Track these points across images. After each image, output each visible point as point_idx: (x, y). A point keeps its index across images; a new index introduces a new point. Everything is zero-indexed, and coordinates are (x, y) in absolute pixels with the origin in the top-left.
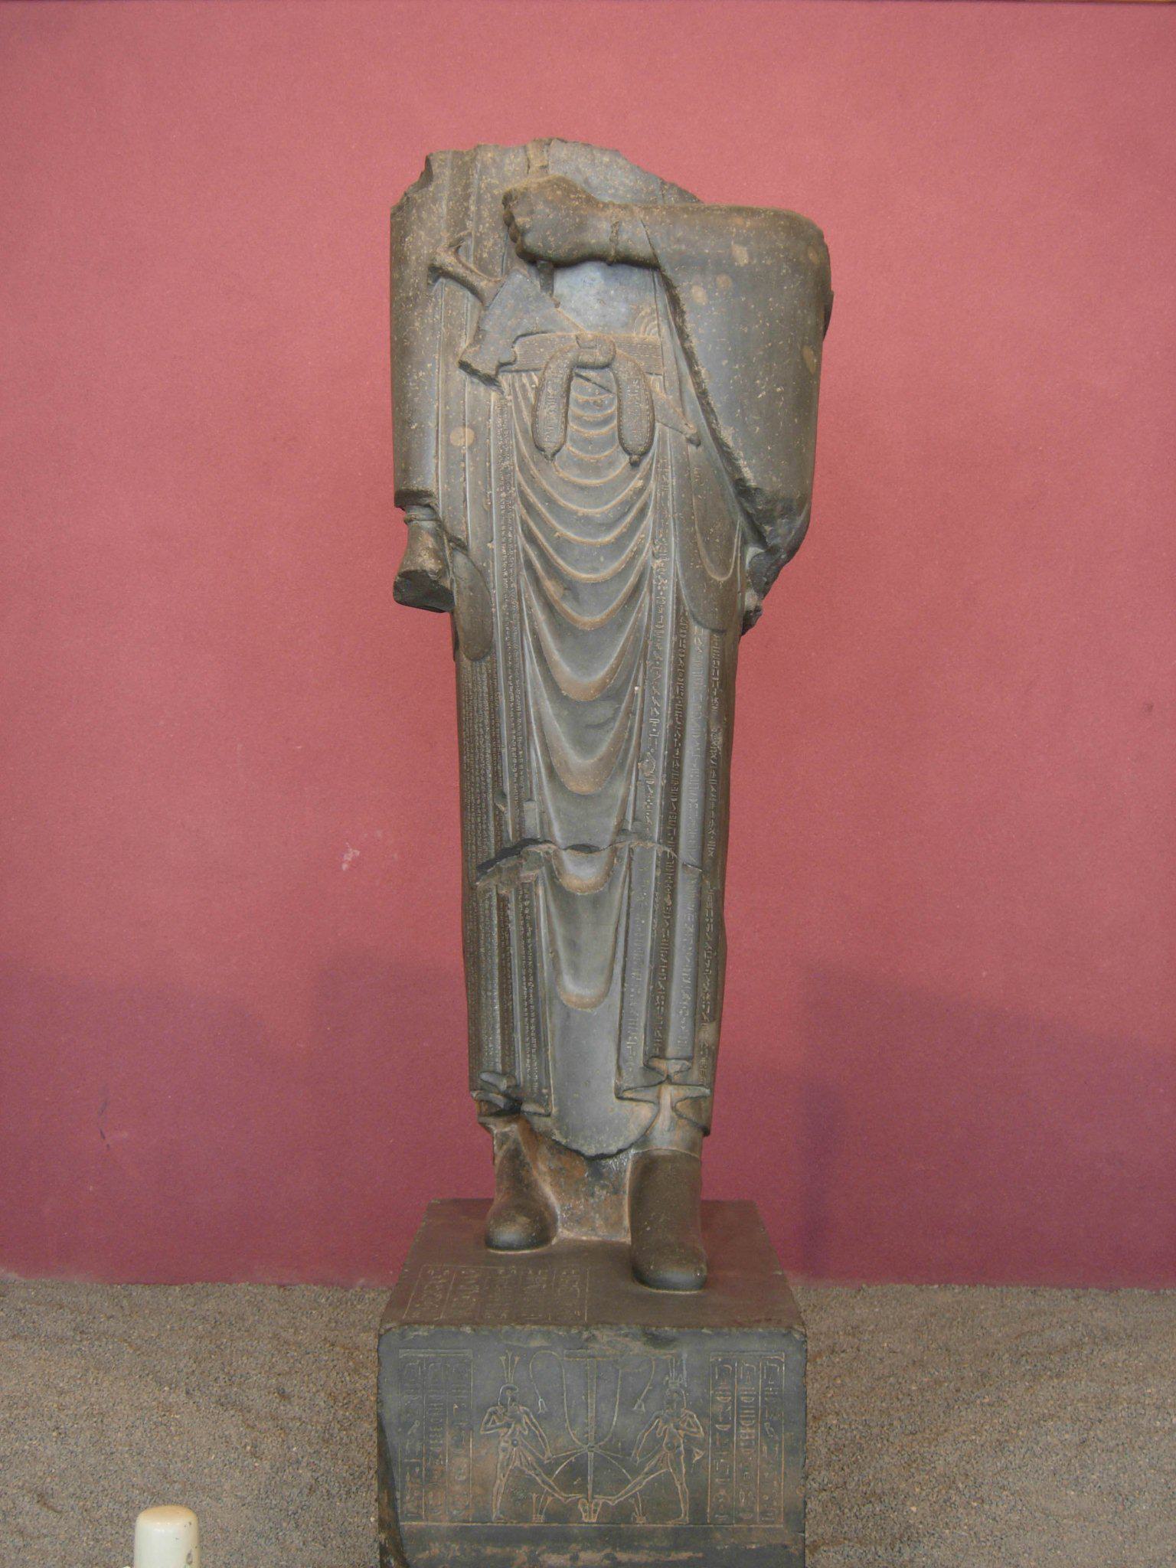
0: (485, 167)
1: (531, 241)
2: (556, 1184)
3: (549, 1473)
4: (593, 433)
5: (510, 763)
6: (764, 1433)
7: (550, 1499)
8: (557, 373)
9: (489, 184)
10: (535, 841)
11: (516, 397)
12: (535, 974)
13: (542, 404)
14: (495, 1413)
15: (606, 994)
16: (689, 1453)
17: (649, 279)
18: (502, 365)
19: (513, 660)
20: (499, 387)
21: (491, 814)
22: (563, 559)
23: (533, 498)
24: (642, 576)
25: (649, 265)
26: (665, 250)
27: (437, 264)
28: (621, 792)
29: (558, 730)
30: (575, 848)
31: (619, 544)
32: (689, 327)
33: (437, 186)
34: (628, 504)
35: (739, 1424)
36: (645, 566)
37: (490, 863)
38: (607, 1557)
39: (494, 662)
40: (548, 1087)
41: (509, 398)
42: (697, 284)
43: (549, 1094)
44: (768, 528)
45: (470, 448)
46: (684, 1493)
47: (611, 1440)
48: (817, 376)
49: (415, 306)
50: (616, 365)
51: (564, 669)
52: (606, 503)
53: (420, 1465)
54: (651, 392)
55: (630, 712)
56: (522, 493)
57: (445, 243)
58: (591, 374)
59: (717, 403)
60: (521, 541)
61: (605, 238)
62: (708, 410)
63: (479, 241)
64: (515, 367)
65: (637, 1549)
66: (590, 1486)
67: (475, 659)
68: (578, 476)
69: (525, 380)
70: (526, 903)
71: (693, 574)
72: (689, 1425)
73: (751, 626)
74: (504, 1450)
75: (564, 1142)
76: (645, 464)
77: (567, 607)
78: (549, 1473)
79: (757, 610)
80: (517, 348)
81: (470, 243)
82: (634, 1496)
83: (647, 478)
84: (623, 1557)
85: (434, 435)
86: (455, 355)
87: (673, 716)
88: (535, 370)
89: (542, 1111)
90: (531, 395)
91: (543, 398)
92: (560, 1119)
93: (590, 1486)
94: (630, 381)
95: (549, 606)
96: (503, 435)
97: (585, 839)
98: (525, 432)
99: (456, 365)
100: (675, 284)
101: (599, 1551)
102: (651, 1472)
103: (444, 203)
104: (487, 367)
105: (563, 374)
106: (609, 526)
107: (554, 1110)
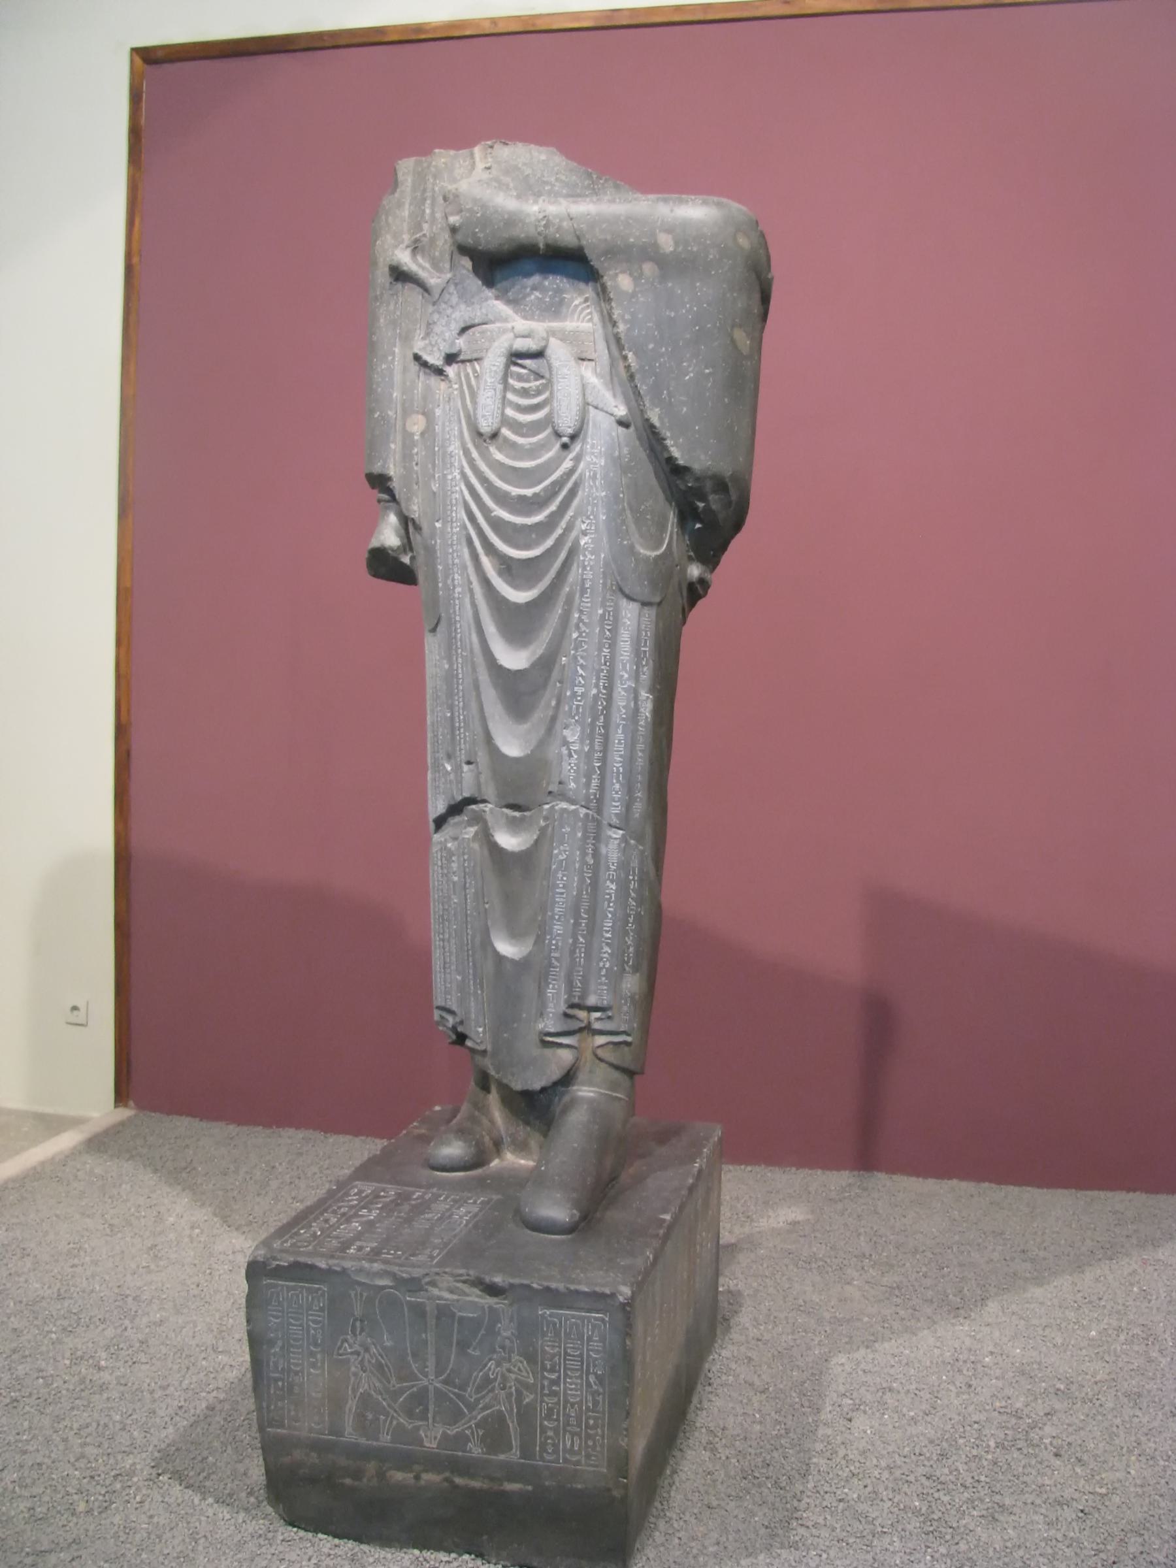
3: (395, 1401)
7: (395, 1423)
8: (494, 361)
20: (447, 376)
23: (474, 480)
27: (394, 263)
32: (616, 313)
35: (566, 1375)
38: (446, 1480)
41: (456, 386)
42: (623, 272)
44: (701, 505)
45: (422, 434)
50: (549, 352)
52: (540, 483)
53: (283, 1380)
58: (527, 362)
61: (532, 232)
63: (433, 240)
64: (462, 357)
65: (472, 1476)
68: (514, 458)
69: (469, 370)
72: (519, 1369)
74: (355, 1374)
76: (576, 448)
79: (703, 583)
83: (578, 459)
86: (411, 347)
88: (476, 360)
91: (482, 387)
93: (430, 1415)
97: (520, 801)
98: (468, 417)
99: (411, 357)
100: (601, 272)
101: (439, 1473)
102: (485, 1408)
103: (407, 206)
104: (435, 359)
105: (501, 361)
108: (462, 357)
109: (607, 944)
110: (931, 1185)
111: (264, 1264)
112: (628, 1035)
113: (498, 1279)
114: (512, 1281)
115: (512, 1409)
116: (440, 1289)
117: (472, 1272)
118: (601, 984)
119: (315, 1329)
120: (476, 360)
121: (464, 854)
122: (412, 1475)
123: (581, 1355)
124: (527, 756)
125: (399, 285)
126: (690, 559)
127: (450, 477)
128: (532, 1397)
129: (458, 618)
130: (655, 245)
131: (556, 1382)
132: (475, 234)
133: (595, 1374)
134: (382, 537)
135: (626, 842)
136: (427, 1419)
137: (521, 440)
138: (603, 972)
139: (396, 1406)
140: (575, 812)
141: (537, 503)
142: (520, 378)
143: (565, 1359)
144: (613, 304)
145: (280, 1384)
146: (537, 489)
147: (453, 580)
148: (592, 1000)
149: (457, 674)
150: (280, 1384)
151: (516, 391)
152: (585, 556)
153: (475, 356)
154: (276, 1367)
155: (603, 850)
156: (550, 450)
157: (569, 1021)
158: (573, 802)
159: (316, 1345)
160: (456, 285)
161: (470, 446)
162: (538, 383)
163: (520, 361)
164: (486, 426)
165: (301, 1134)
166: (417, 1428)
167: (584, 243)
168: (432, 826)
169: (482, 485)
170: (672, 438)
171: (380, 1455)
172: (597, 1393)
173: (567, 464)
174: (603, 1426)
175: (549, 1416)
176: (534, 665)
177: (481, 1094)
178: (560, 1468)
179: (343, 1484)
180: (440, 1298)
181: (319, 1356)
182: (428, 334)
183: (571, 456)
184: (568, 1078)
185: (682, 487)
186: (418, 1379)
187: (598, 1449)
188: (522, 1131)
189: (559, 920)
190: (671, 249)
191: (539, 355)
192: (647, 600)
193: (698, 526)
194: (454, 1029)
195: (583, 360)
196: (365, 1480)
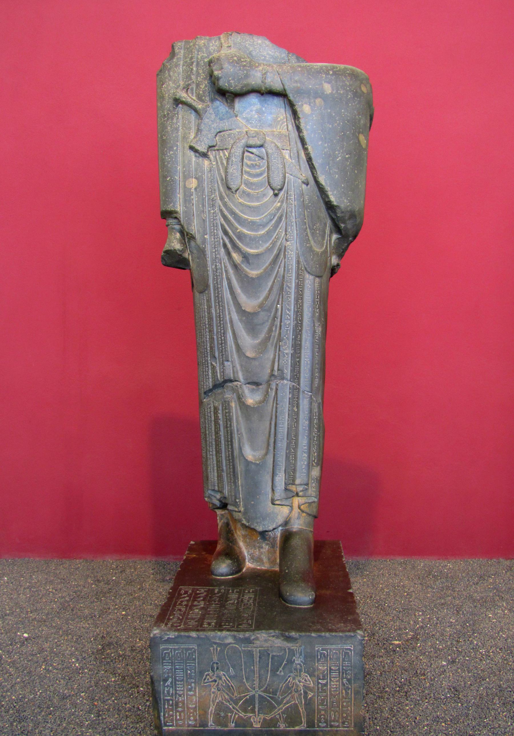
0: (200, 48)
1: (223, 84)
2: (245, 542)
3: (236, 704)
4: (255, 180)
5: (218, 343)
6: (343, 684)
7: (237, 716)
9: (203, 56)
10: (231, 381)
11: (217, 163)
12: (232, 445)
13: (230, 166)
14: (208, 675)
15: (266, 454)
16: (306, 693)
17: (282, 102)
18: (210, 147)
19: (218, 292)
20: (209, 158)
21: (210, 367)
22: (242, 243)
23: (226, 213)
24: (280, 250)
25: (282, 95)
26: (290, 87)
27: (177, 97)
28: (272, 357)
29: (240, 327)
30: (249, 383)
31: (269, 234)
32: (302, 126)
33: (178, 58)
35: (330, 679)
37: (211, 390)
39: (209, 294)
41: (214, 163)
42: (306, 104)
43: (240, 502)
45: (196, 189)
47: (267, 688)
49: (168, 119)
51: (242, 298)
52: (262, 215)
53: (172, 700)
55: (275, 317)
56: (221, 211)
59: (317, 163)
60: (221, 233)
62: (312, 167)
63: (198, 85)
64: (216, 148)
66: (257, 710)
67: (201, 292)
68: (248, 202)
69: (222, 154)
72: (305, 680)
73: (335, 273)
74: (213, 693)
77: (244, 267)
78: (236, 704)
79: (338, 265)
80: (217, 138)
81: (194, 86)
82: (279, 714)
83: (282, 202)
85: (178, 182)
88: (226, 149)
89: (236, 509)
90: (225, 162)
91: (230, 163)
92: (245, 513)
93: (257, 710)
95: (235, 266)
96: (211, 182)
97: (255, 379)
98: (222, 180)
99: (188, 147)
100: (295, 103)
102: (287, 703)
104: (202, 148)
105: (240, 150)
106: (264, 226)
107: (242, 509)
111: (161, 638)
128: (312, 694)
129: (219, 286)
131: (326, 685)
139: (237, 708)
142: (250, 159)
143: (330, 672)
150: (171, 702)
151: (248, 166)
152: (288, 252)
153: (225, 147)
161: (224, 194)
163: (250, 150)
169: (231, 215)
170: (331, 191)
181: (193, 685)
186: (248, 691)
187: (349, 718)
190: (330, 92)
192: (318, 275)
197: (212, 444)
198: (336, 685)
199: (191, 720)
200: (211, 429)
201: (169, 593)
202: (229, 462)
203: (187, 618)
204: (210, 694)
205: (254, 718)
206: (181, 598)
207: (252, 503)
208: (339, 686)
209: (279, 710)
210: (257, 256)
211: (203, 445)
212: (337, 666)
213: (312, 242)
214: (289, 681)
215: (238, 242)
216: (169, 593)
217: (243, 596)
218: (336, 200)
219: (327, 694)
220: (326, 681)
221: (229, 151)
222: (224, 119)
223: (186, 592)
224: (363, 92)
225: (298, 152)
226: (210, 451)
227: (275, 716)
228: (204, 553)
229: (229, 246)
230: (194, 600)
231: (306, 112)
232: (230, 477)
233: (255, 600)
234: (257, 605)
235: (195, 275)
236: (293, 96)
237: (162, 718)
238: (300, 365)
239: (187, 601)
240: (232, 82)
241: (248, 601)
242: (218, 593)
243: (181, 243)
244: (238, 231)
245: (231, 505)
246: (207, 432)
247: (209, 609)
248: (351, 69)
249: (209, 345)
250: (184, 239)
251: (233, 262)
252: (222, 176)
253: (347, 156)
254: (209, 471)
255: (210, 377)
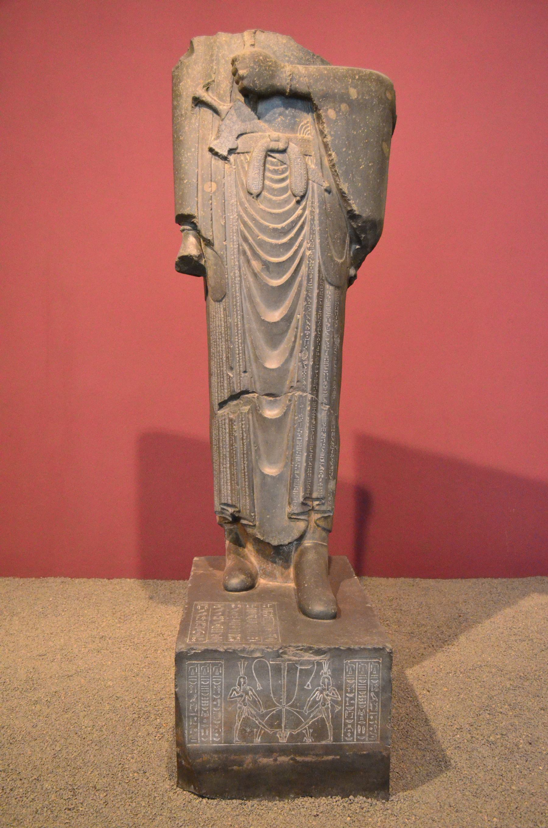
7: (263, 732)
8: (258, 154)
20: (229, 161)
23: (246, 219)
27: (197, 96)
34: (295, 223)
35: (358, 694)
36: (304, 253)
38: (292, 759)
40: (254, 512)
41: (234, 167)
42: (330, 108)
43: (255, 516)
46: (330, 726)
47: (294, 702)
48: (388, 158)
49: (186, 119)
50: (289, 150)
51: (262, 307)
52: (284, 221)
53: (197, 717)
54: (307, 165)
56: (240, 216)
57: (202, 86)
58: (277, 155)
62: (335, 175)
63: (218, 85)
64: (238, 151)
68: (270, 208)
70: (243, 423)
71: (327, 260)
72: (333, 694)
73: (351, 284)
74: (240, 708)
75: (262, 539)
76: (303, 203)
83: (304, 209)
84: (299, 759)
87: (316, 330)
88: (247, 152)
89: (251, 524)
92: (261, 526)
93: (283, 725)
94: (296, 158)
95: (255, 275)
97: (273, 391)
101: (287, 756)
102: (314, 717)
103: (200, 64)
107: (257, 523)
108: (238, 151)
109: (322, 465)
110: (391, 580)
111: (187, 653)
112: (331, 512)
113: (322, 646)
114: (329, 647)
115: (329, 716)
116: (289, 656)
117: (305, 644)
118: (319, 486)
119: (216, 686)
120: (247, 152)
121: (242, 421)
122: (271, 759)
123: (367, 683)
124: (279, 368)
125: (197, 108)
126: (352, 265)
127: (232, 217)
128: (340, 708)
130: (348, 94)
132: (254, 81)
133: (374, 691)
134: (189, 250)
135: (330, 412)
136: (281, 727)
137: (274, 198)
138: (321, 480)
139: (263, 723)
140: (306, 396)
141: (284, 232)
142: (272, 164)
144: (325, 125)
145: (196, 719)
146: (284, 224)
147: (235, 273)
148: (315, 495)
149: (237, 325)
150: (196, 719)
151: (270, 171)
153: (246, 150)
154: (193, 709)
155: (319, 416)
156: (289, 204)
157: (304, 507)
158: (304, 391)
159: (217, 694)
160: (235, 110)
162: (283, 167)
163: (272, 155)
164: (255, 190)
165: (59, 580)
166: (275, 733)
167: (311, 90)
168: (216, 407)
169: (252, 222)
170: (353, 200)
171: (254, 750)
172: (375, 701)
173: (299, 211)
174: (378, 718)
175: (349, 718)
176: (282, 319)
177: (240, 549)
178: (355, 744)
179: (232, 769)
180: (290, 660)
181: (219, 701)
182: (218, 137)
183: (301, 207)
184: (301, 538)
185: (355, 226)
186: (275, 706)
187: (375, 731)
188: (270, 567)
189: (298, 454)
190: (356, 97)
191: (284, 151)
193: (358, 247)
194: (232, 515)
195: (306, 155)
196: (245, 766)
197: (226, 457)
198: (364, 698)
199: (215, 737)
200: (225, 441)
201: (186, 609)
202: (245, 475)
203: (210, 633)
204: (237, 710)
205: (280, 734)
206: (199, 613)
207: (268, 516)
208: (367, 699)
209: (306, 725)
210: (279, 264)
211: (215, 457)
212: (365, 679)
213: (333, 252)
214: (317, 696)
215: (258, 249)
216: (186, 609)
217: (262, 610)
218: (358, 209)
219: (355, 708)
220: (353, 694)
221: (250, 154)
222: (246, 121)
223: (202, 608)
224: (387, 99)
225: (321, 159)
226: (223, 464)
227: (302, 731)
228: (211, 569)
229: (249, 253)
230: (212, 616)
231: (331, 117)
232: (245, 490)
233: (275, 614)
234: (278, 619)
235: (211, 282)
236: (319, 99)
237: (186, 735)
238: (318, 378)
239: (206, 616)
240: (257, 82)
241: (268, 616)
242: (236, 607)
243: (198, 249)
244: (259, 237)
245: (245, 519)
246: (221, 445)
247: (230, 624)
248: (376, 74)
249: (225, 355)
250: (201, 246)
251: (253, 270)
252: (242, 180)
253: (370, 164)
254: (222, 484)
255: (225, 387)
